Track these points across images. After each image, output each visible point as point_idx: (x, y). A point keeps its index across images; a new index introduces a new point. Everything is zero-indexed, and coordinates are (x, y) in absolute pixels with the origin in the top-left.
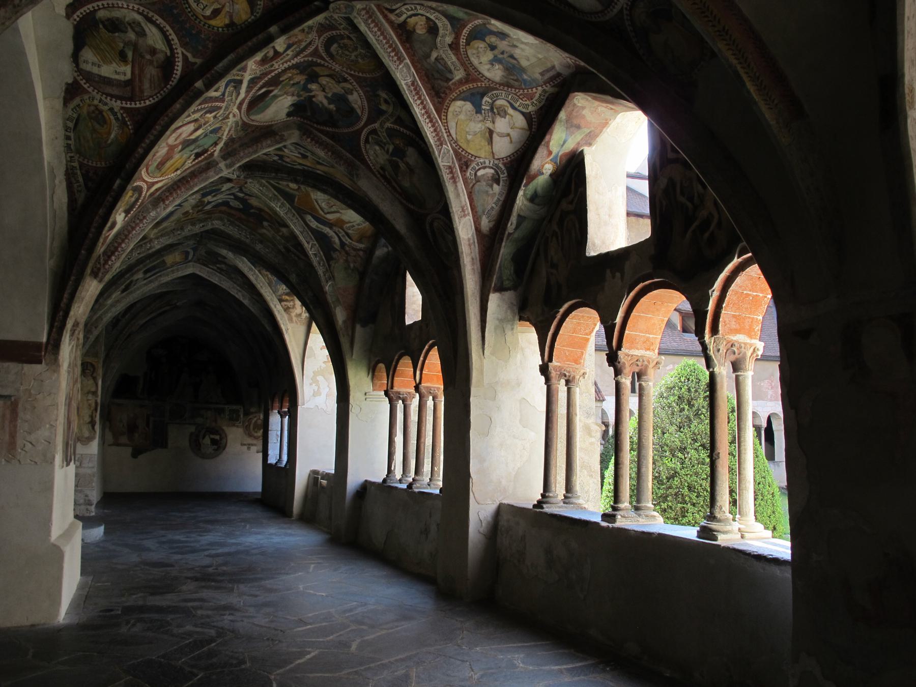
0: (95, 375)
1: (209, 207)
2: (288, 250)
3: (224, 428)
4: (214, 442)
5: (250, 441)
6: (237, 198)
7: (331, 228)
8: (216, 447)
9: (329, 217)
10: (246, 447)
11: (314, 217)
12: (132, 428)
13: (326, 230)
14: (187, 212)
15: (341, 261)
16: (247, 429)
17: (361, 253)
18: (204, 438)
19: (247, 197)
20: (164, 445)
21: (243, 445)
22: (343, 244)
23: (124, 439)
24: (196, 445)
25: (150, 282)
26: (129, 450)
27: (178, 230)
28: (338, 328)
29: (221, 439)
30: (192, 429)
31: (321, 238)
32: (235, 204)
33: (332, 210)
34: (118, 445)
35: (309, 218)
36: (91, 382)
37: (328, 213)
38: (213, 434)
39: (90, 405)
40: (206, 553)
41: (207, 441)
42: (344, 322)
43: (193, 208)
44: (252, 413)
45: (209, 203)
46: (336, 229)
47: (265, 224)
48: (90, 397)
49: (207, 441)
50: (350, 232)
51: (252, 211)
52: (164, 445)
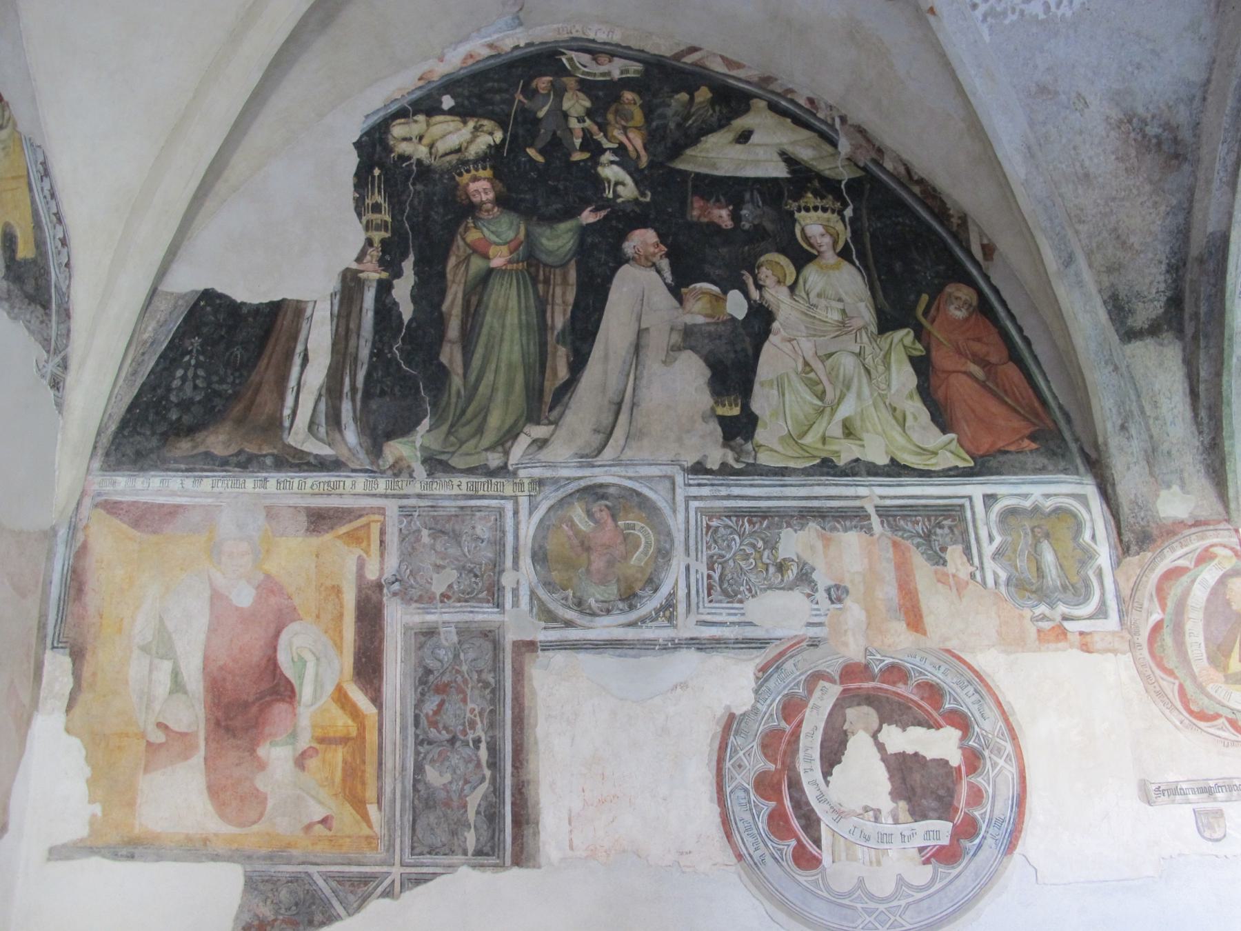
3: (988, 661)
5: (1200, 754)
8: (940, 830)
10: (1181, 814)
12: (246, 702)
16: (1161, 647)
18: (832, 755)
20: (507, 832)
21: (1153, 793)
23: (178, 797)
24: (780, 815)
29: (974, 760)
30: (732, 684)
34: (132, 848)
38: (895, 712)
41: (862, 779)
44: (1173, 530)
49: (862, 779)
52: (507, 832)
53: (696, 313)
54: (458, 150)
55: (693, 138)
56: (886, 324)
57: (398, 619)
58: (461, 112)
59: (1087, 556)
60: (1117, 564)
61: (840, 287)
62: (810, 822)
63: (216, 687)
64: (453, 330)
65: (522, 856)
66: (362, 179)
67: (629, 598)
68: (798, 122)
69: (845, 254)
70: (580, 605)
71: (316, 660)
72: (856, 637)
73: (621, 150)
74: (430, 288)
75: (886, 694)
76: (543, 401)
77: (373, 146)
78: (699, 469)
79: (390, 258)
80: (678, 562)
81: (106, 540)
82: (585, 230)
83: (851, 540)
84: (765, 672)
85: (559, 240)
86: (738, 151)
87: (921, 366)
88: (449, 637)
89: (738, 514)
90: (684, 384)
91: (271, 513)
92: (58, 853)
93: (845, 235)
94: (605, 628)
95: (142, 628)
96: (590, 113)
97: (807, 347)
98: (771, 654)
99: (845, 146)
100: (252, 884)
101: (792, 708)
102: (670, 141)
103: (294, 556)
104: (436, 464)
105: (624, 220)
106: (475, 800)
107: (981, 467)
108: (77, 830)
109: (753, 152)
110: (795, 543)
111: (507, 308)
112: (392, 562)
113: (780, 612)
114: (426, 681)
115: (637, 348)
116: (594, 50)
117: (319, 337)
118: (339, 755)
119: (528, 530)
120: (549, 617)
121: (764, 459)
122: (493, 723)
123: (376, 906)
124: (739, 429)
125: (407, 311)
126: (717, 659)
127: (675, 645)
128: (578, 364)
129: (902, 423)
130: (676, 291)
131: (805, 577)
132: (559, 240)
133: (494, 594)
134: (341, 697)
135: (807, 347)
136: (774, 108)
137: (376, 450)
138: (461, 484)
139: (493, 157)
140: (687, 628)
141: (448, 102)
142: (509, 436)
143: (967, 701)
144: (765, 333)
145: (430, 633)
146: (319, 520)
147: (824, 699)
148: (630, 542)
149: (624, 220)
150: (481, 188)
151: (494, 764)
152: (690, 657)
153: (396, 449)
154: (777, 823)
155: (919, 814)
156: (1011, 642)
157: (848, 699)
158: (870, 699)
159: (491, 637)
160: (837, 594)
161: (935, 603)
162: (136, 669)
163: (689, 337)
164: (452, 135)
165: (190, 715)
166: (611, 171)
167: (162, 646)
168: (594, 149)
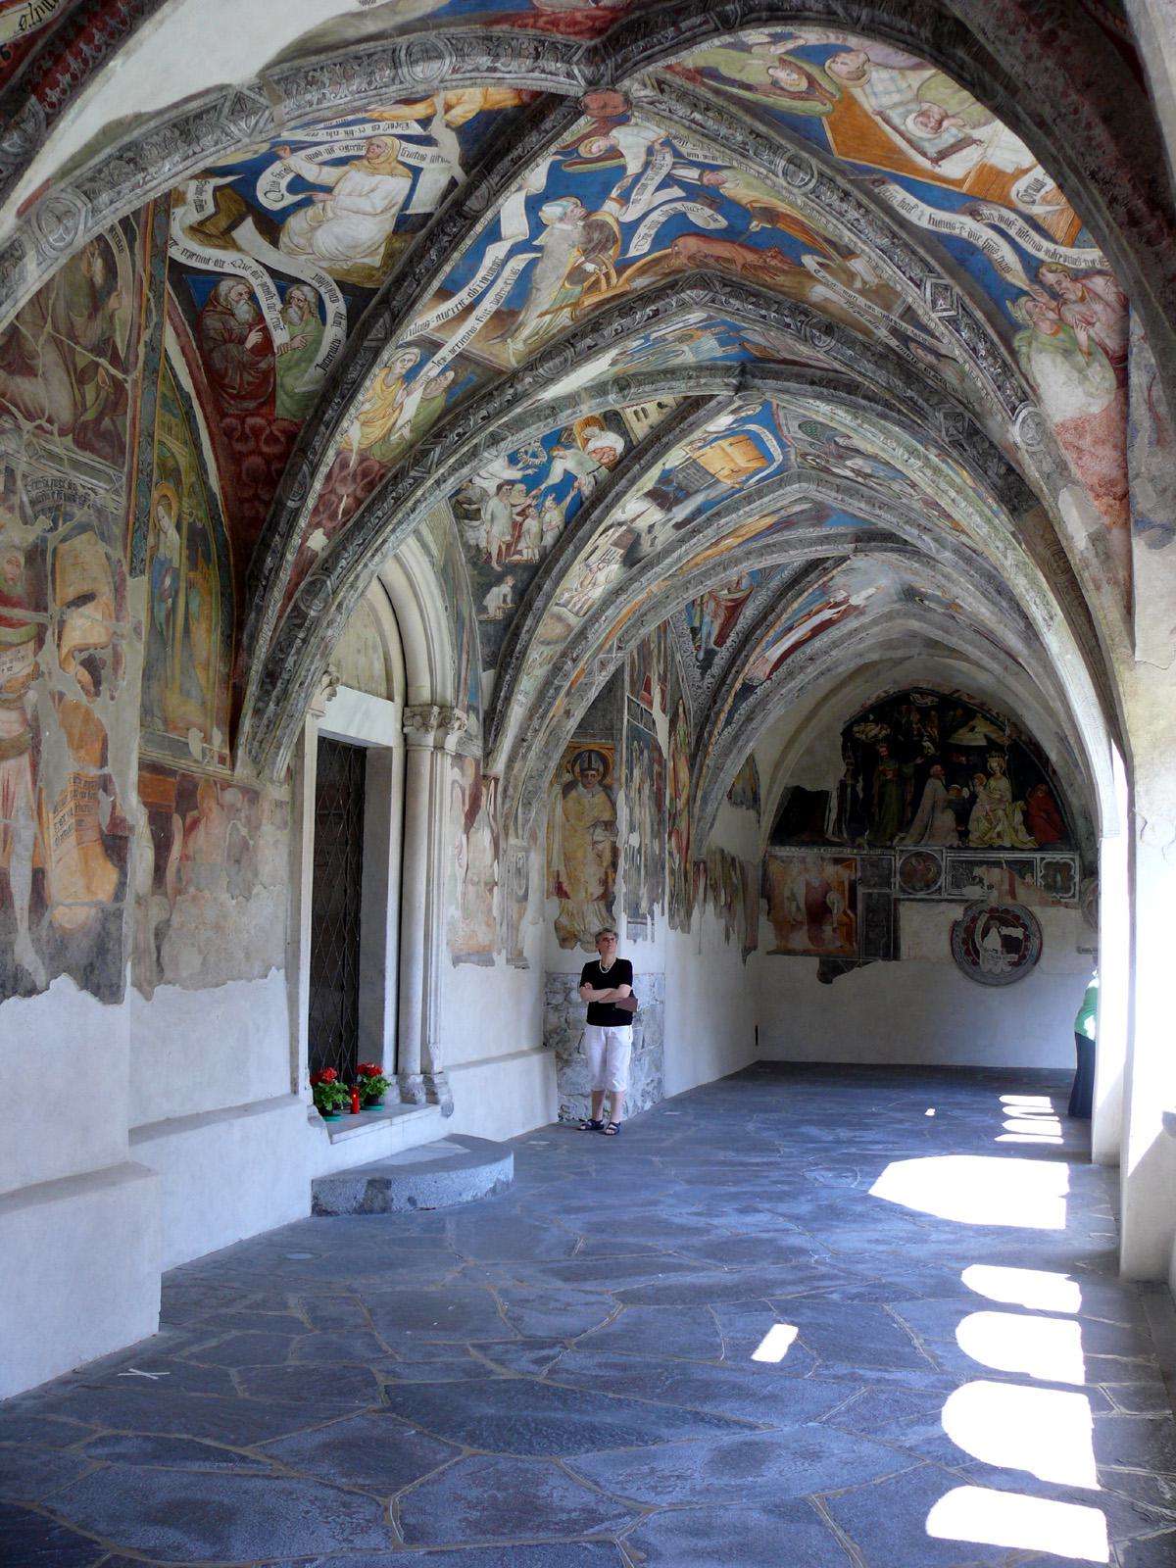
0: (608, 781)
1: (639, 246)
2: (905, 339)
3: (1036, 910)
4: (1010, 945)
6: (693, 192)
7: (974, 214)
8: (1015, 957)
9: (954, 168)
11: (910, 186)
12: (818, 912)
13: (963, 225)
14: (576, 275)
15: (1045, 327)
17: (1098, 283)
18: (985, 933)
19: (709, 178)
20: (891, 952)
22: (1032, 266)
23: (800, 939)
25: (695, 532)
26: (814, 963)
27: (584, 336)
28: (1075, 560)
29: (1027, 938)
30: (957, 913)
31: (960, 260)
32: (701, 215)
33: (948, 138)
34: (789, 952)
35: (897, 194)
36: (600, 797)
37: (943, 155)
38: (1006, 923)
39: (599, 856)
40: (639, 1283)
41: (993, 941)
42: (1096, 539)
43: (586, 252)
45: (630, 229)
46: (991, 212)
47: (809, 261)
48: (600, 834)
49: (993, 941)
50: (1037, 210)
51: (755, 226)
52: (891, 952)
53: (952, 796)
54: (876, 736)
55: (955, 730)
56: (1015, 799)
57: (861, 890)
58: (876, 722)
59: (1072, 878)
60: (1081, 881)
61: (1001, 785)
62: (977, 952)
63: (809, 907)
64: (876, 801)
65: (896, 957)
66: (844, 748)
67: (928, 886)
68: (992, 723)
69: (1004, 774)
70: (914, 888)
71: (837, 902)
72: (993, 900)
73: (930, 736)
74: (867, 788)
75: (1003, 917)
76: (904, 825)
77: (847, 733)
78: (951, 847)
79: (854, 773)
80: (943, 876)
81: (774, 868)
82: (917, 765)
83: (996, 871)
84: (966, 910)
85: (908, 769)
86: (970, 735)
87: (1025, 813)
88: (875, 896)
89: (962, 862)
90: (947, 819)
91: (823, 859)
92: (769, 953)
93: (1004, 766)
94: (920, 895)
95: (787, 893)
96: (919, 721)
97: (988, 807)
98: (969, 904)
99: (1008, 731)
100: (822, 963)
101: (974, 920)
102: (948, 730)
103: (831, 871)
104: (872, 845)
105: (930, 761)
106: (884, 940)
107: (1041, 848)
108: (773, 947)
109: (975, 736)
110: (978, 871)
111: (892, 792)
112: (859, 874)
113: (973, 892)
114: (868, 909)
115: (933, 808)
116: (922, 692)
117: (834, 803)
118: (844, 929)
119: (898, 865)
120: (904, 891)
121: (972, 845)
122: (888, 921)
123: (856, 969)
124: (964, 834)
125: (861, 795)
126: (953, 905)
127: (942, 901)
128: (914, 814)
129: (1016, 832)
130: (947, 787)
131: (981, 881)
132: (908, 769)
133: (889, 885)
134: (845, 912)
135: (988, 807)
136: (984, 717)
137: (854, 842)
138: (879, 851)
139: (886, 738)
140: (945, 896)
141: (871, 717)
142: (891, 839)
143: (1028, 922)
144: (974, 803)
145: (870, 895)
146: (837, 861)
147: (984, 918)
148: (929, 870)
149: (930, 761)
150: (883, 751)
151: (888, 932)
152: (944, 906)
153: (859, 840)
154: (968, 952)
155: (1008, 952)
156: (1044, 904)
157: (991, 918)
158: (997, 918)
159: (888, 896)
160: (990, 887)
161: (1021, 891)
162: (786, 903)
163: (949, 804)
164: (874, 730)
165: (802, 916)
166: (927, 744)
167: (793, 897)
168: (921, 735)
